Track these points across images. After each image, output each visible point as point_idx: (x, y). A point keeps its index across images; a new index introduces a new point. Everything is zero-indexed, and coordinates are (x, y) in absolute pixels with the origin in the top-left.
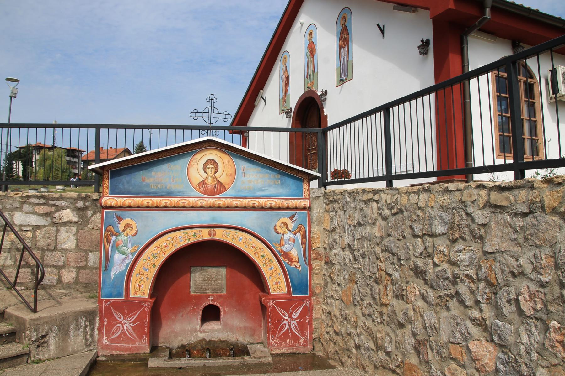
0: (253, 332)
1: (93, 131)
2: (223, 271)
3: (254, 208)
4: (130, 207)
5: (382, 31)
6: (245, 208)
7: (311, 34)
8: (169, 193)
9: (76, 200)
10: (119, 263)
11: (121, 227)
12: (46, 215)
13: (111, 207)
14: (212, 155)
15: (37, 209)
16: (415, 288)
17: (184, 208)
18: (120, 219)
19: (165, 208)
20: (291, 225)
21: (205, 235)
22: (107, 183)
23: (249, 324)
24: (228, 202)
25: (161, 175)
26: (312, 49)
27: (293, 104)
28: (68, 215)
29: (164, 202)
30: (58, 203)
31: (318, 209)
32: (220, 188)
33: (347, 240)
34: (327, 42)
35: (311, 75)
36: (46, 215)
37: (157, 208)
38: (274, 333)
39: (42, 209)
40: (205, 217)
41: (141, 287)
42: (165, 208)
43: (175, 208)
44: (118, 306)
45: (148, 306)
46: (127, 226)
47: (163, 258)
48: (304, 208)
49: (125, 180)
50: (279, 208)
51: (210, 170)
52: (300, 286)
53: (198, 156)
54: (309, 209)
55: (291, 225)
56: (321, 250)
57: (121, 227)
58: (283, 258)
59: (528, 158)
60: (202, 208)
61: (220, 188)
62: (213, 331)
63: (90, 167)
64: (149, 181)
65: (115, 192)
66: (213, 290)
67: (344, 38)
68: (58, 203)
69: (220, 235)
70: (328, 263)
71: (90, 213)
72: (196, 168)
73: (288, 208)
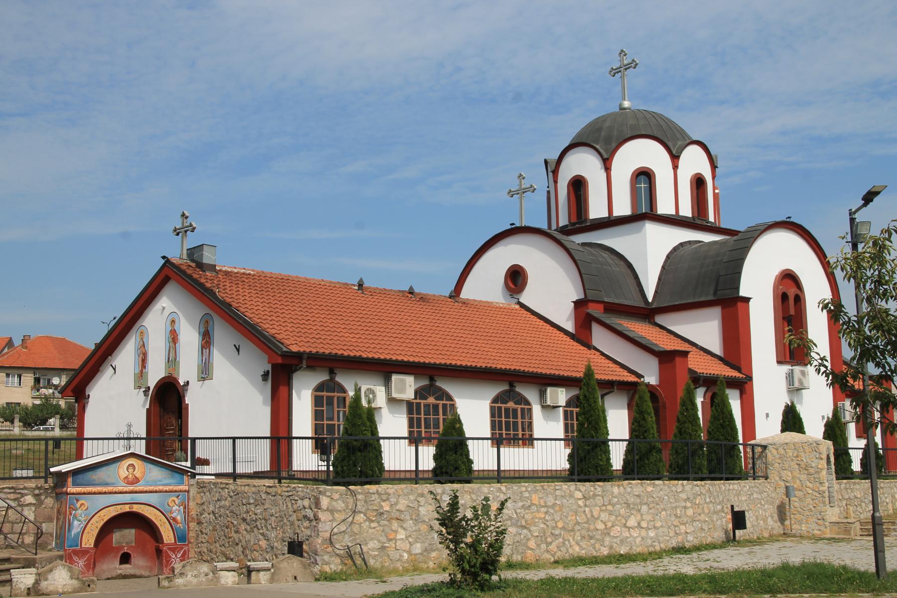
0: (151, 569)
1: (43, 442)
2: (133, 531)
3: (156, 492)
4: (84, 494)
5: (238, 350)
6: (151, 492)
7: (173, 321)
8: (107, 484)
9: (34, 489)
10: (77, 526)
11: (78, 505)
12: (15, 500)
13: (73, 494)
14: (132, 461)
15: (10, 496)
16: (243, 526)
17: (116, 493)
18: (77, 500)
19: (105, 493)
20: (177, 501)
21: (127, 509)
22: (70, 480)
23: (149, 564)
24: (141, 488)
25: (102, 474)
26: (174, 337)
27: (152, 383)
28: (29, 499)
29: (104, 489)
30: (23, 492)
31: (193, 491)
32: (136, 480)
33: (211, 508)
34: (190, 337)
35: (172, 361)
36: (15, 500)
37: (100, 493)
38: (166, 567)
39: (12, 496)
40: (127, 498)
41: (89, 541)
42: (105, 493)
43: (110, 493)
44: (76, 553)
45: (93, 551)
46: (82, 504)
47: (102, 523)
48: (185, 491)
49: (80, 476)
50: (171, 492)
51: (131, 470)
52: (181, 537)
53: (124, 462)
54: (188, 492)
55: (177, 501)
56: (194, 516)
57: (78, 505)
58: (172, 521)
59: (284, 474)
60: (126, 492)
61: (136, 480)
62: (126, 568)
63: (52, 470)
64: (94, 477)
65: (75, 484)
66: (127, 543)
67: (207, 340)
68: (23, 492)
69: (136, 508)
70: (199, 523)
71: (43, 497)
72: (122, 470)
73: (176, 491)
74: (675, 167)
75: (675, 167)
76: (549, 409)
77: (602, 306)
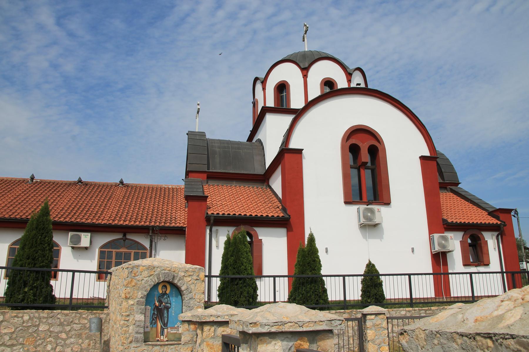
74: (305, 76)
75: (305, 76)
76: (76, 249)
77: (205, 175)
